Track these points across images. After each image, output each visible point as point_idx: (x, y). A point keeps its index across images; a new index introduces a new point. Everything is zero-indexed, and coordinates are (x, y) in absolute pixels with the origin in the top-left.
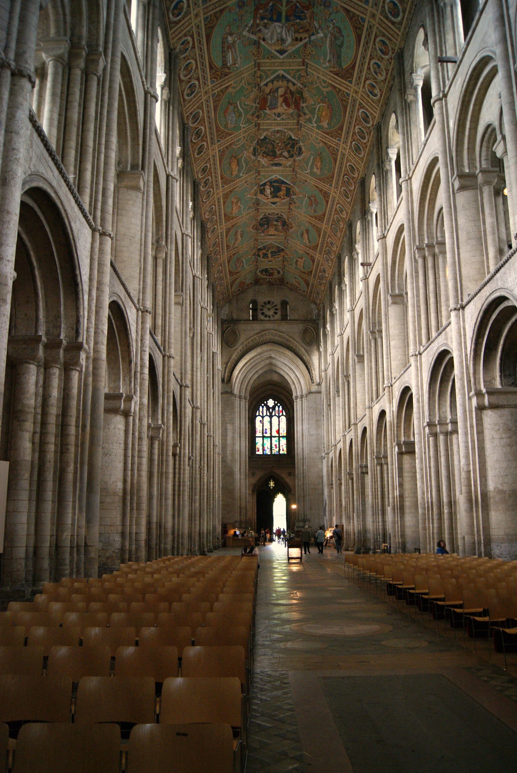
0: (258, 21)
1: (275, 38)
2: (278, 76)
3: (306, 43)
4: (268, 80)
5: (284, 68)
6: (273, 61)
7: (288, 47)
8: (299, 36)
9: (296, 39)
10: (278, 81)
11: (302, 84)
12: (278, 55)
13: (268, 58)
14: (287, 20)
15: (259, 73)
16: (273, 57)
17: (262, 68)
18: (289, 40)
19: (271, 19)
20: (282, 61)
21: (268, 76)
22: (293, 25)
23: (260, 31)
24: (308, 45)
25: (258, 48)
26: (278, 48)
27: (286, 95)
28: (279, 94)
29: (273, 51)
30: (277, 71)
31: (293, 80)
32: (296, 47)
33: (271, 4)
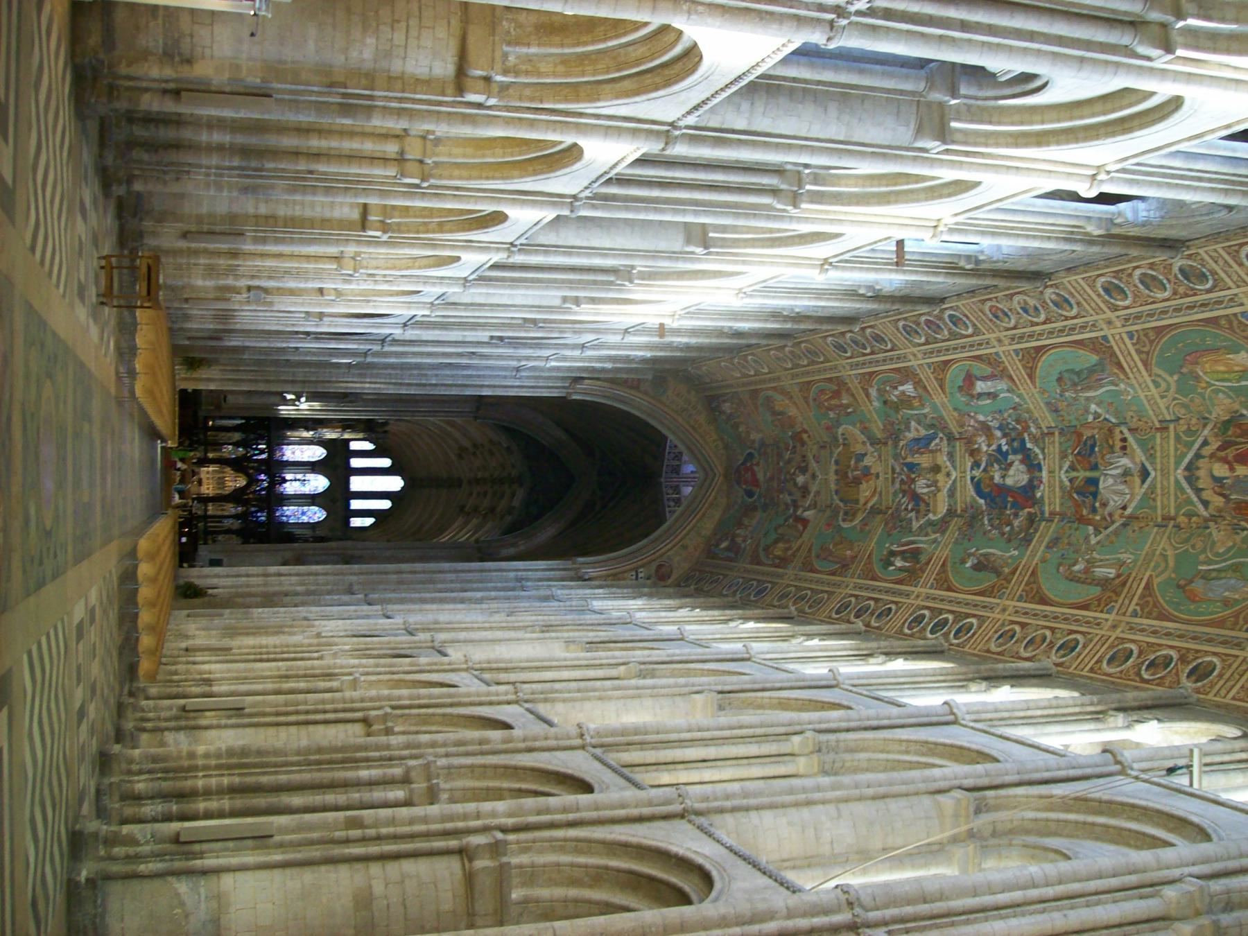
0: (1098, 518)
1: (1122, 487)
2: (1186, 478)
3: (1130, 430)
4: (1195, 499)
5: (1172, 466)
6: (1159, 491)
7: (1135, 463)
8: (1118, 444)
9: (1124, 448)
10: (1198, 478)
11: (1205, 426)
12: (1149, 480)
13: (1154, 500)
14: (1095, 467)
15: (1182, 519)
16: (1152, 488)
17: (1173, 513)
18: (1125, 461)
19: (1095, 495)
20: (1159, 473)
21: (1188, 501)
22: (1102, 458)
23: (1111, 515)
24: (1133, 425)
25: (1137, 518)
26: (1137, 480)
27: (1230, 458)
28: (1227, 474)
29: (1143, 490)
30: (1177, 482)
31: (1197, 446)
32: (1135, 447)
33: (1075, 496)
